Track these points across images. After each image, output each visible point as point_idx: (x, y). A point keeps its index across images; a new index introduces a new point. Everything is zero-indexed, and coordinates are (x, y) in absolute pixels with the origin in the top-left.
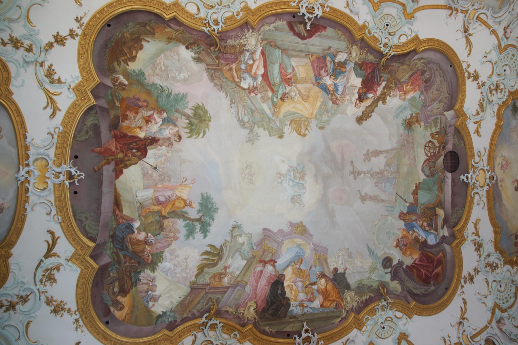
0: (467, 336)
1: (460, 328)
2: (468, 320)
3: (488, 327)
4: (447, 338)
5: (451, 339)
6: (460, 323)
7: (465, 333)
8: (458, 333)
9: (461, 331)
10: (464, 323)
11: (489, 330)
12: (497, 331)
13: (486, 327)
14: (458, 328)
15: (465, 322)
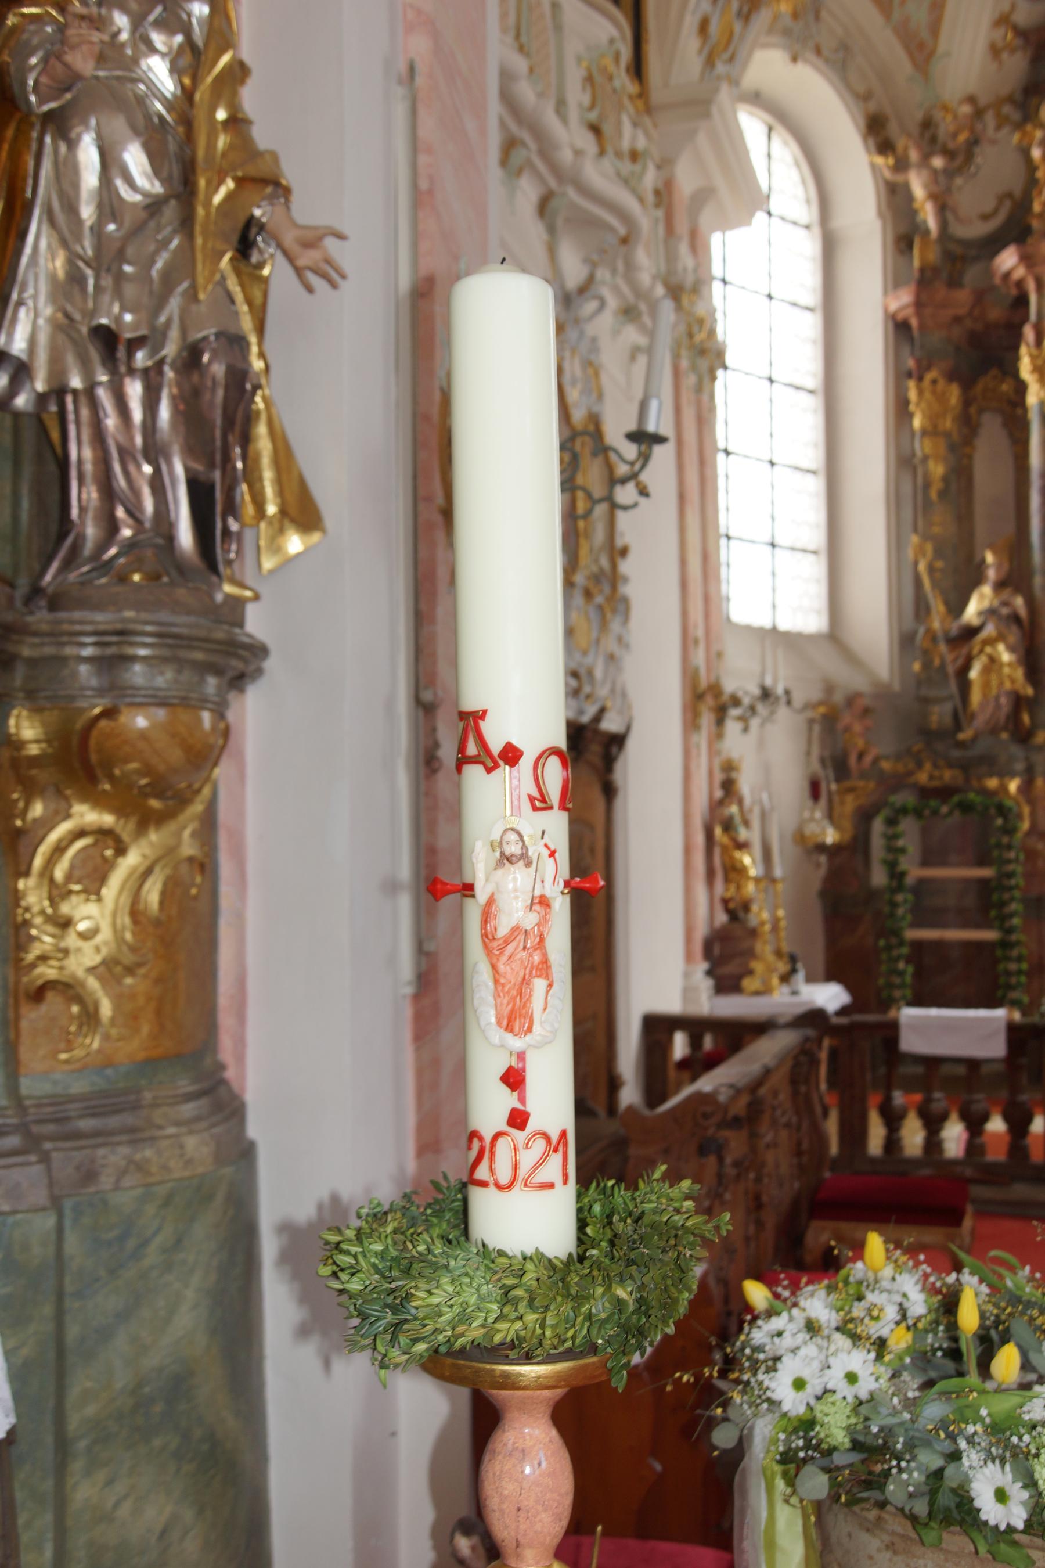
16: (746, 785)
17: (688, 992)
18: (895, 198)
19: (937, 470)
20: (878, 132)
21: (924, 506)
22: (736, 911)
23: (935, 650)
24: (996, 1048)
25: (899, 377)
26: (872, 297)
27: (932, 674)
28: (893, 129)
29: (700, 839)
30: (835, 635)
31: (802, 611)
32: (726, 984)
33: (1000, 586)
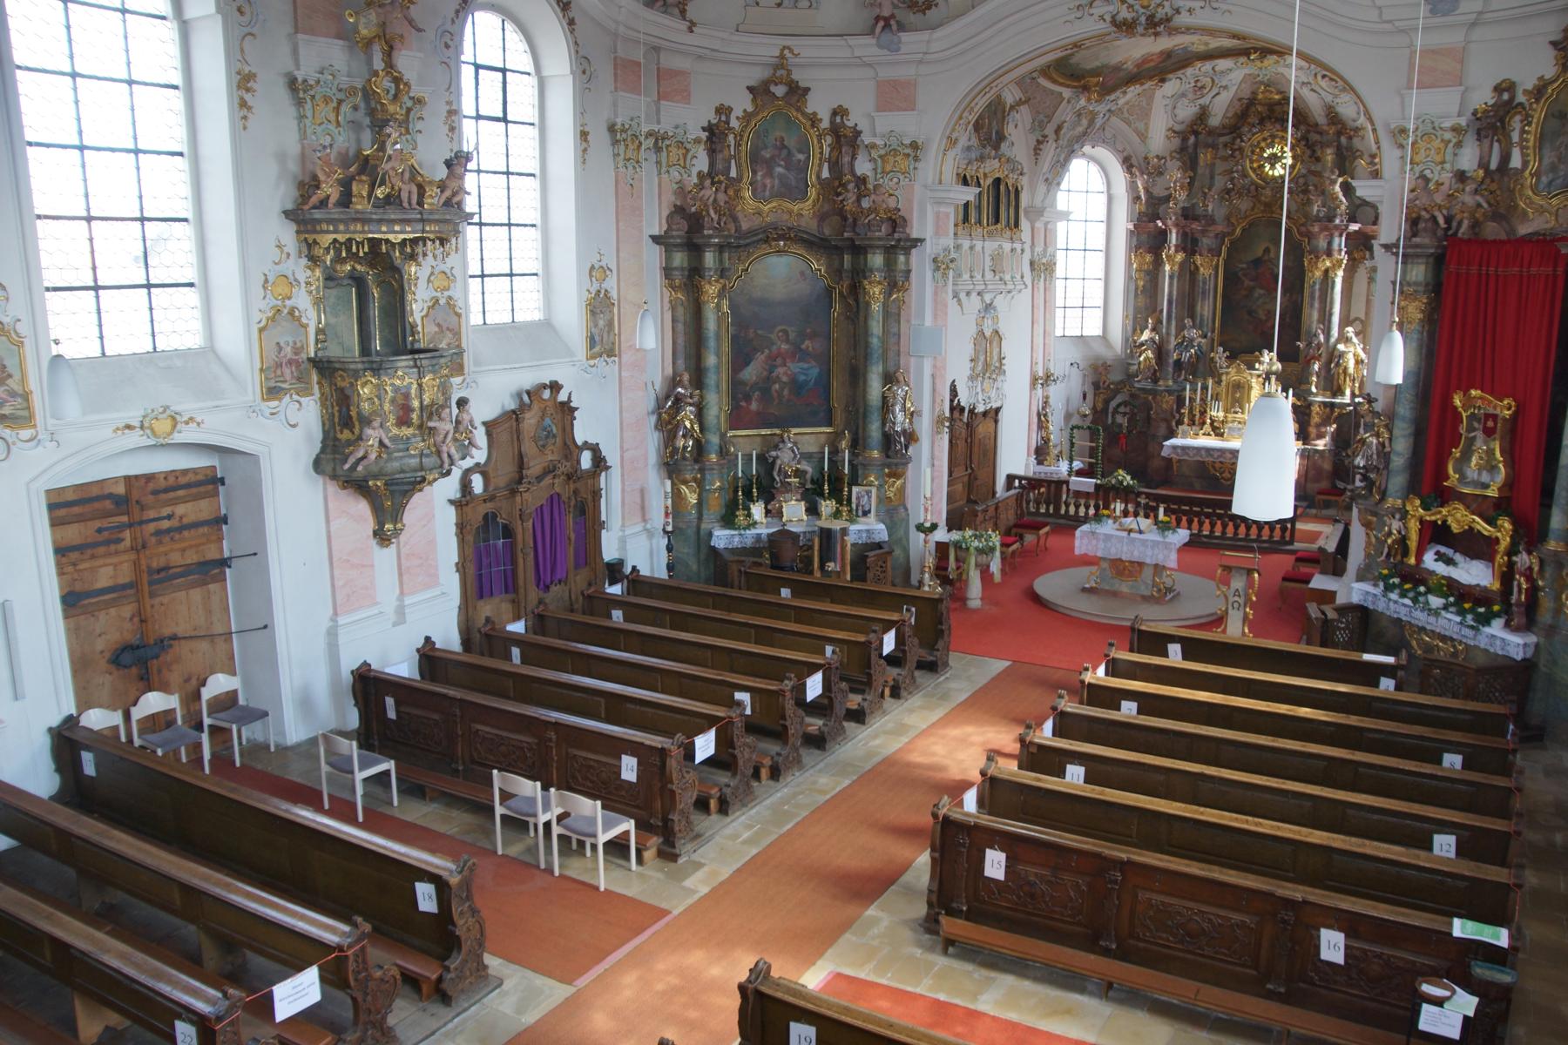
16: (1051, 401)
17: (1027, 466)
18: (1132, 187)
19: (1141, 283)
20: (1127, 163)
21: (1136, 295)
22: (1046, 441)
23: (1134, 347)
24: (1092, 490)
25: (1130, 249)
26: (1123, 225)
27: (1132, 355)
28: (1134, 161)
29: (1035, 420)
30: (1104, 338)
31: (1093, 328)
32: (1040, 463)
33: (1153, 330)
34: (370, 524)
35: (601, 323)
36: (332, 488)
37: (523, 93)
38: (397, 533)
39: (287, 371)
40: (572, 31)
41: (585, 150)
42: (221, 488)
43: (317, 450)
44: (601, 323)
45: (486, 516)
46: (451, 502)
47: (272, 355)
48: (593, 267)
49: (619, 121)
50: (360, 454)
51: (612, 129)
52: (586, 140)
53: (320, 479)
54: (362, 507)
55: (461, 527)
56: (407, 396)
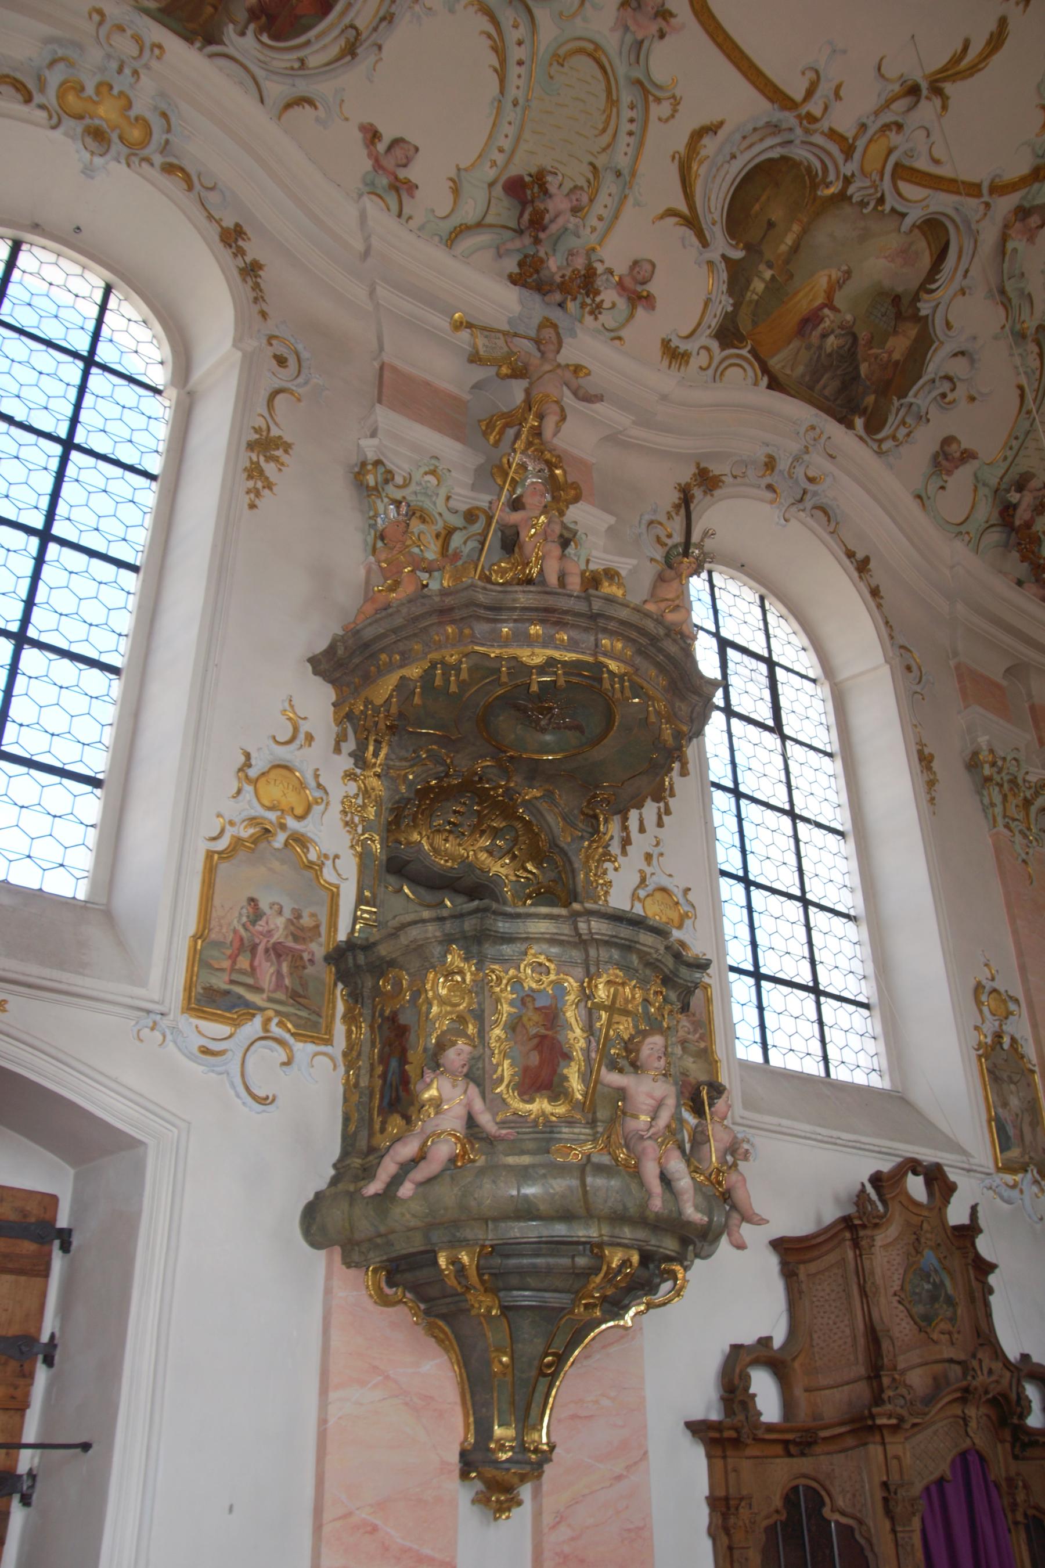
0: (890, 151)
1: (894, 106)
2: (944, 107)
3: (979, 195)
4: (825, 89)
5: (837, 108)
6: (913, 91)
7: (894, 138)
8: (876, 113)
9: (888, 117)
10: (923, 103)
11: (972, 205)
12: (989, 235)
13: (973, 189)
14: (887, 104)
15: (927, 109)
34: (454, 1432)
35: (1014, 1102)
36: (354, 1289)
37: (807, 710)
38: (533, 1463)
39: (267, 972)
40: (879, 606)
41: (931, 784)
42: (58, 1262)
43: (322, 1184)
44: (1014, 1102)
45: (791, 1498)
46: (697, 1429)
47: (231, 918)
48: (979, 988)
49: (983, 740)
50: (407, 1150)
51: (973, 764)
52: (929, 768)
53: (319, 1263)
54: (436, 1373)
55: (723, 1506)
56: (552, 1016)
